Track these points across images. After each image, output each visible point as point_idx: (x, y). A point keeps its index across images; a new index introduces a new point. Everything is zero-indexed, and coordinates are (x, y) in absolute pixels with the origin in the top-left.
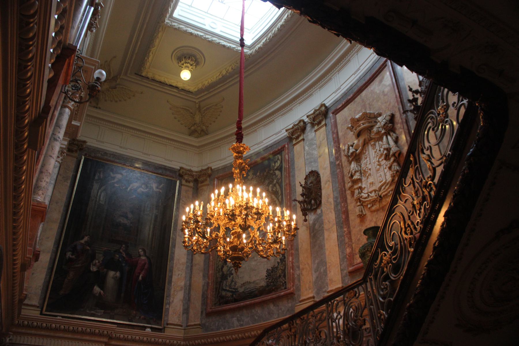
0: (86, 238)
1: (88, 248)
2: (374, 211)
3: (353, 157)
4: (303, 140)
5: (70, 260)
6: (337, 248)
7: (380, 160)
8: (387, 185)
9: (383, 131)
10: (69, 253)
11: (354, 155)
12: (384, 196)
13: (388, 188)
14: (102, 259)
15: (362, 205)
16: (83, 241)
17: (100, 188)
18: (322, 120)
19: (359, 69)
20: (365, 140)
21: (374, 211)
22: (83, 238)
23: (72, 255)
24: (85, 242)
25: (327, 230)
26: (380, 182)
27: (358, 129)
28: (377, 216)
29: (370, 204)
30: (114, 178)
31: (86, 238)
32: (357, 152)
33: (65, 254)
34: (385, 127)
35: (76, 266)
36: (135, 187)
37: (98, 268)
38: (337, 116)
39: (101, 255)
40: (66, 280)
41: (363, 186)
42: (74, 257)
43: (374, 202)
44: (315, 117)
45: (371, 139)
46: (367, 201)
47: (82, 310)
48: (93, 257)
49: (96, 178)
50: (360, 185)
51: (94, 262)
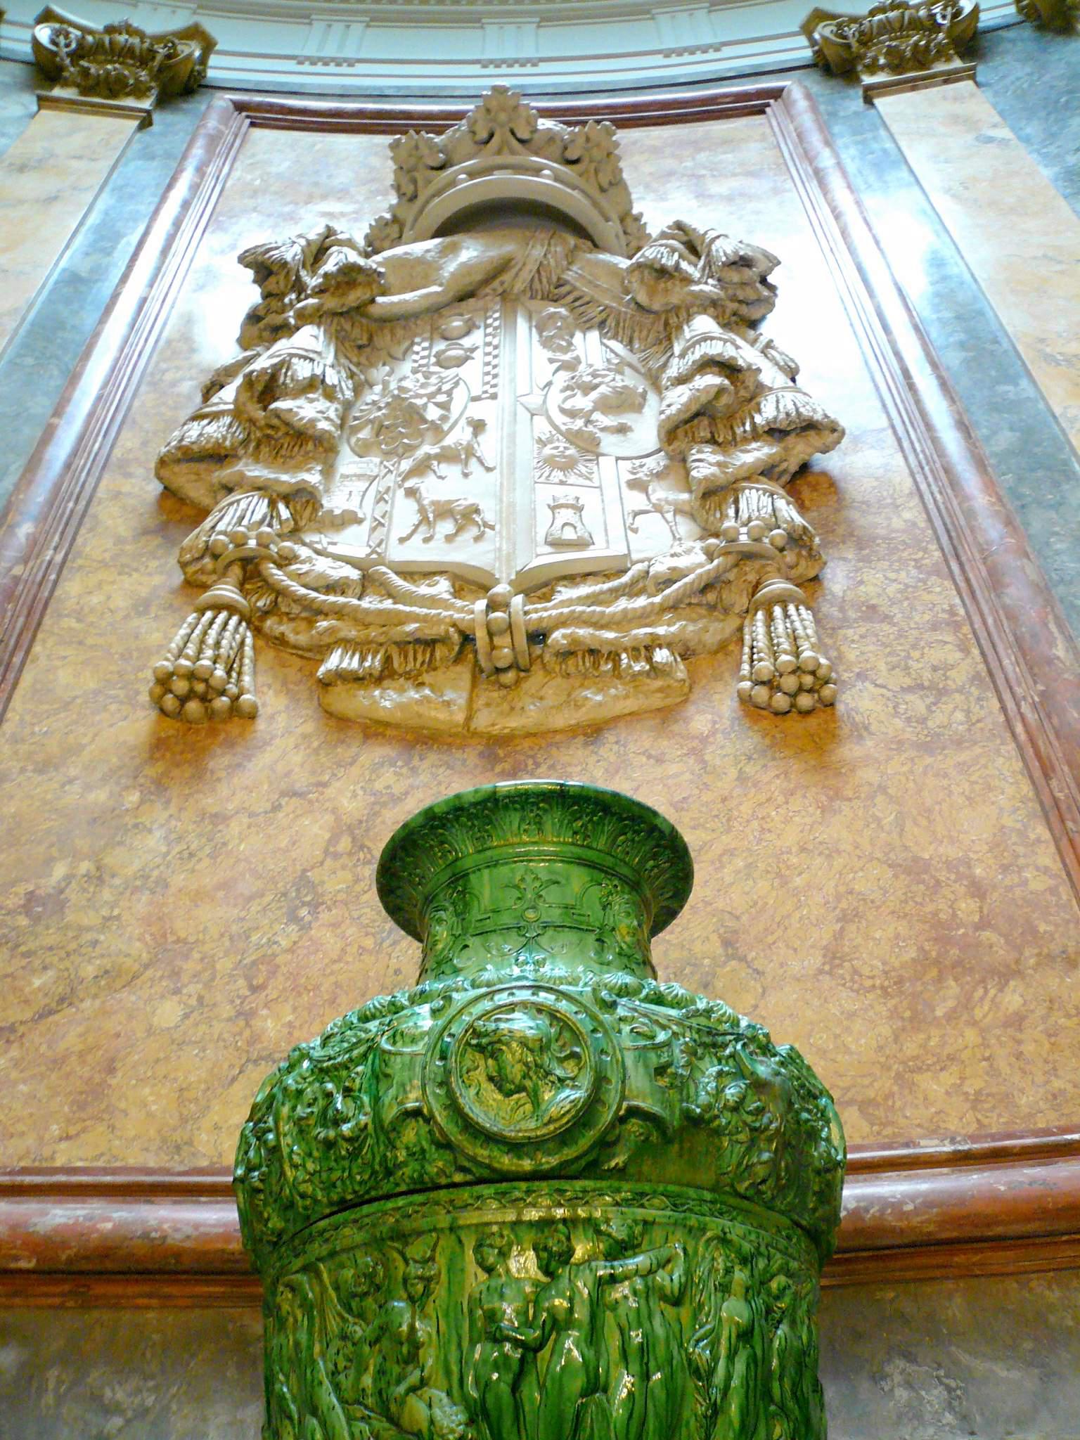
2: (374, 729)
3: (331, 303)
8: (632, 590)
9: (709, 287)
11: (355, 297)
13: (644, 617)
15: (253, 620)
18: (139, 92)
20: (502, 268)
21: (374, 729)
27: (504, 184)
29: (360, 647)
32: (380, 299)
34: (734, 276)
38: (257, 133)
43: (414, 654)
44: (99, 46)
45: (556, 291)
46: (338, 612)
50: (313, 477)
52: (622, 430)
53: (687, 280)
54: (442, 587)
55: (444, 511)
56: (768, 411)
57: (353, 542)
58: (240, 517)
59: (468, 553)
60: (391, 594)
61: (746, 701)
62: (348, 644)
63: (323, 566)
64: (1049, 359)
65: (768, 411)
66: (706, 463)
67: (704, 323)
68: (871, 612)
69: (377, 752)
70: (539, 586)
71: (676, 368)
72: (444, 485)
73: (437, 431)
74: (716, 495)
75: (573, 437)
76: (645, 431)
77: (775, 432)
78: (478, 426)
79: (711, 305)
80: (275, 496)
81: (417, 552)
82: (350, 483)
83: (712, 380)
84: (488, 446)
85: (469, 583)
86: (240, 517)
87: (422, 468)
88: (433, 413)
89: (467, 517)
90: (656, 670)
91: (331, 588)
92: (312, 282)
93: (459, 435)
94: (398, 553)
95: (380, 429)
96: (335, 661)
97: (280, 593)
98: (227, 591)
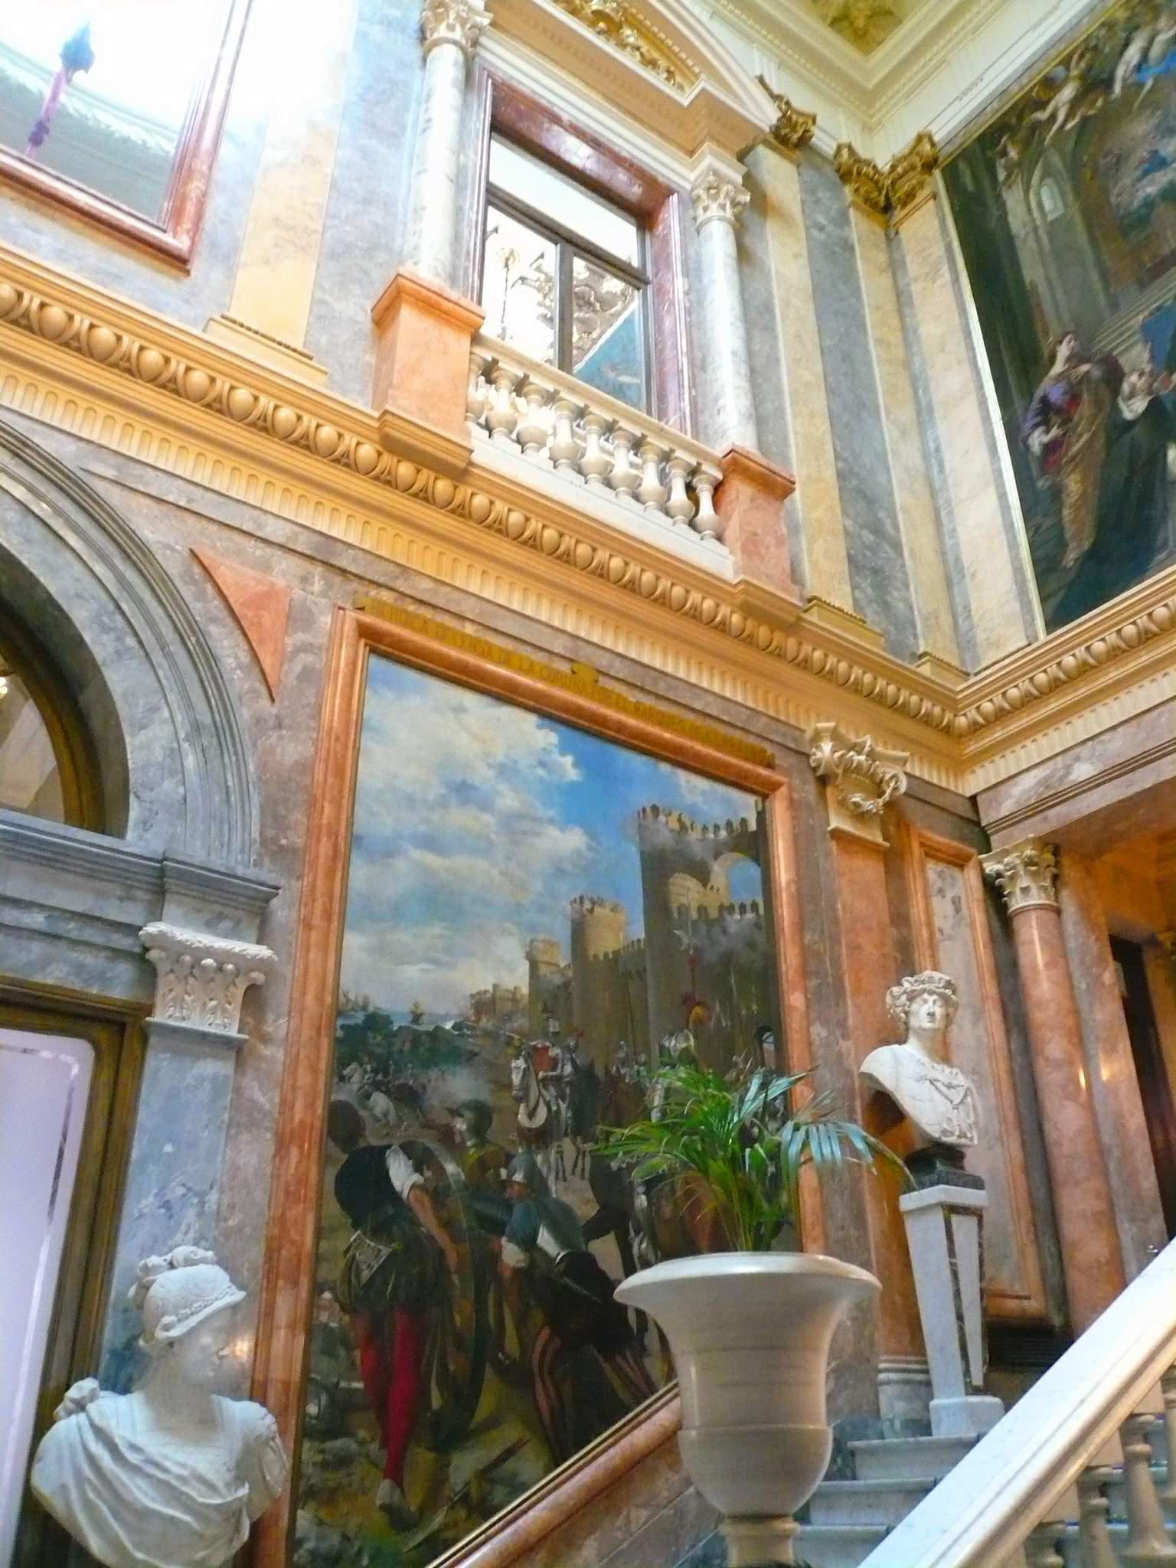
0: (1063, 351)
1: (1085, 368)
5: (1050, 448)
10: (1036, 434)
14: (1146, 356)
16: (1058, 367)
17: (1027, 191)
22: (1052, 360)
23: (1047, 432)
24: (1069, 359)
30: (1053, 117)
31: (1063, 351)
33: (1027, 447)
35: (1075, 449)
36: (1134, 62)
37: (1150, 393)
39: (1139, 347)
40: (1066, 512)
42: (1055, 432)
47: (1162, 556)
48: (1114, 375)
49: (1002, 175)
51: (1126, 388)
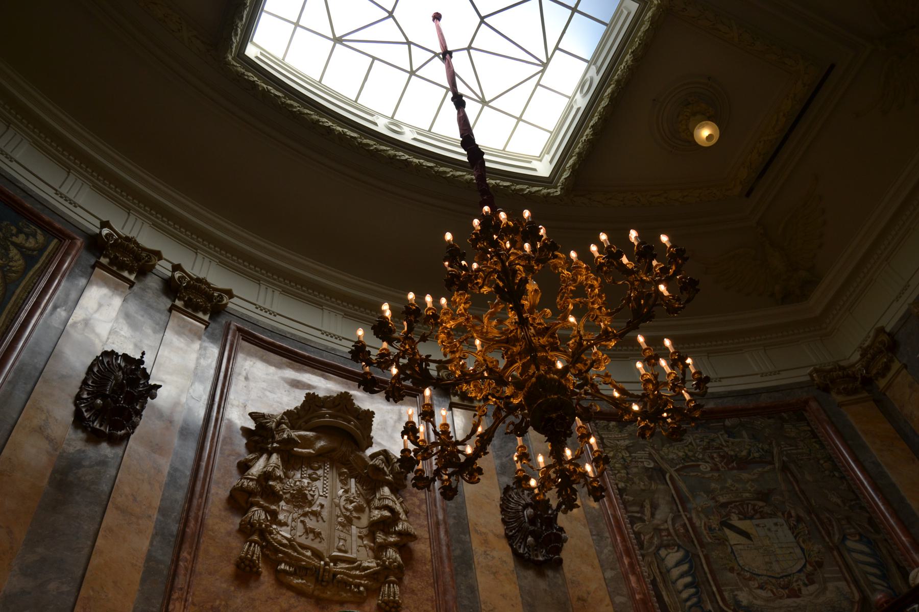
2: (290, 587)
4: (132, 284)
6: (138, 577)
7: (355, 514)
8: (357, 568)
9: (390, 478)
12: (339, 581)
15: (262, 547)
19: (341, 338)
21: (290, 587)
25: (117, 508)
26: (340, 550)
28: (292, 601)
41: (281, 517)
43: (301, 570)
52: (359, 518)
53: (385, 474)
54: (309, 553)
55: (312, 531)
56: (400, 527)
57: (285, 532)
58: (258, 514)
59: (316, 545)
60: (296, 550)
61: (378, 605)
62: (286, 563)
63: (279, 537)
64: (476, 531)
65: (400, 527)
66: (380, 538)
67: (386, 491)
68: (413, 592)
69: (290, 594)
70: (336, 560)
71: (377, 503)
72: (311, 523)
73: (311, 504)
74: (383, 547)
75: (346, 517)
76: (364, 521)
77: (399, 534)
78: (322, 506)
79: (388, 484)
80: (267, 511)
81: (303, 540)
82: (285, 512)
83: (386, 513)
84: (325, 514)
85: (317, 555)
86: (258, 514)
87: (305, 515)
88: (310, 498)
89: (317, 535)
90: (360, 592)
91: (284, 545)
92: (277, 437)
93: (315, 508)
94: (299, 540)
95: (292, 495)
96: (283, 566)
97: (268, 542)
98: (256, 538)
